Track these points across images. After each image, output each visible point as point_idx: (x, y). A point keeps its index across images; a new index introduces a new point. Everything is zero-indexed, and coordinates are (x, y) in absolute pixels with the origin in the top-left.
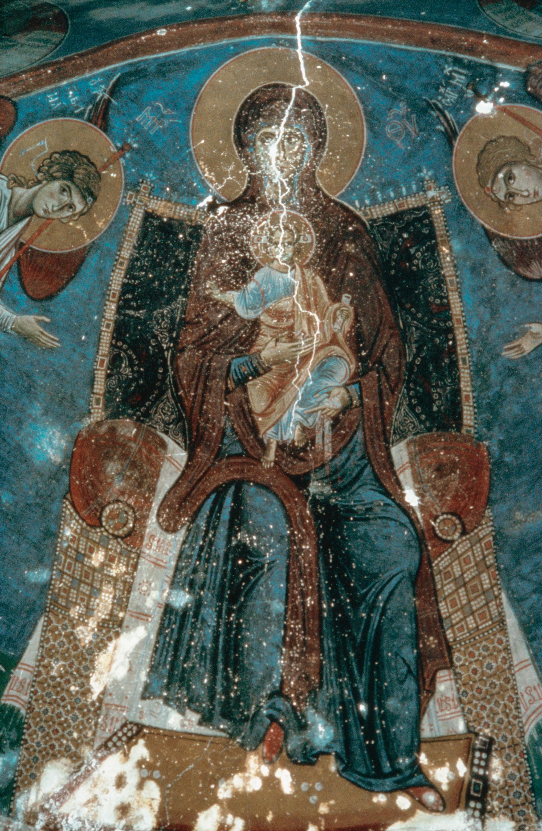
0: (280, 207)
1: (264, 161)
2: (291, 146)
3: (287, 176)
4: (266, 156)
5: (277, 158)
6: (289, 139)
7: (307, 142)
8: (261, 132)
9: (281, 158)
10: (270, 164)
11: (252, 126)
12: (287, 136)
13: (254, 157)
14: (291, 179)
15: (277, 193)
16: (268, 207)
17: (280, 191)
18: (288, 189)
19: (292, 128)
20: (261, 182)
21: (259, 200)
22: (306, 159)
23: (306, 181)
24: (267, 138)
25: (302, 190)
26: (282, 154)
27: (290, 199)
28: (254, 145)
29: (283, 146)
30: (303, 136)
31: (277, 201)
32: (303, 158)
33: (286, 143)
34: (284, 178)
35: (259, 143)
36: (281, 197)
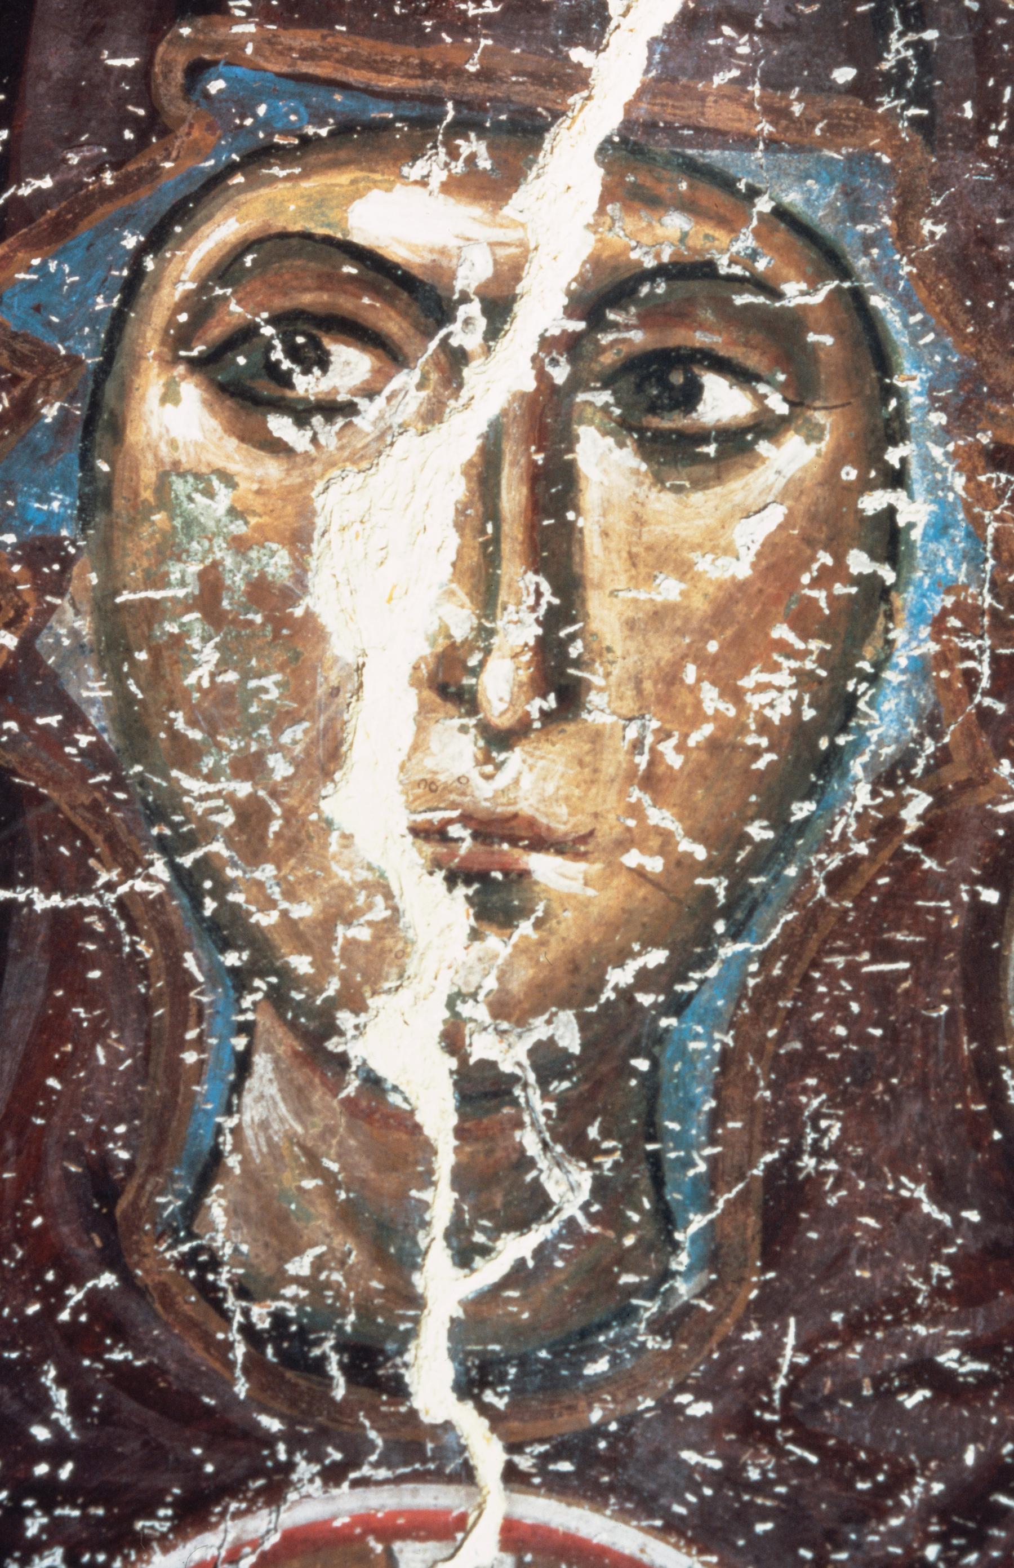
0: (423, 1452)
1: (223, 708)
2: (680, 513)
3: (573, 982)
4: (273, 622)
5: (448, 682)
6: (653, 395)
7: (926, 449)
8: (221, 232)
9: (501, 682)
10: (327, 757)
11: (85, 98)
12: (628, 335)
13: (72, 623)
14: (617, 1031)
15: (388, 1238)
16: (232, 1434)
17: (441, 1202)
18: (569, 1187)
19: (722, 195)
20: (157, 1049)
21: (106, 1318)
22: (886, 720)
23: (853, 1081)
24: (311, 334)
25: (785, 1200)
26: (519, 629)
27: (580, 1343)
28: (100, 421)
29: (555, 486)
30: (873, 349)
31: (374, 1364)
32: (839, 710)
33: (604, 462)
34: (508, 1010)
35: (173, 418)
36: (444, 1287)
